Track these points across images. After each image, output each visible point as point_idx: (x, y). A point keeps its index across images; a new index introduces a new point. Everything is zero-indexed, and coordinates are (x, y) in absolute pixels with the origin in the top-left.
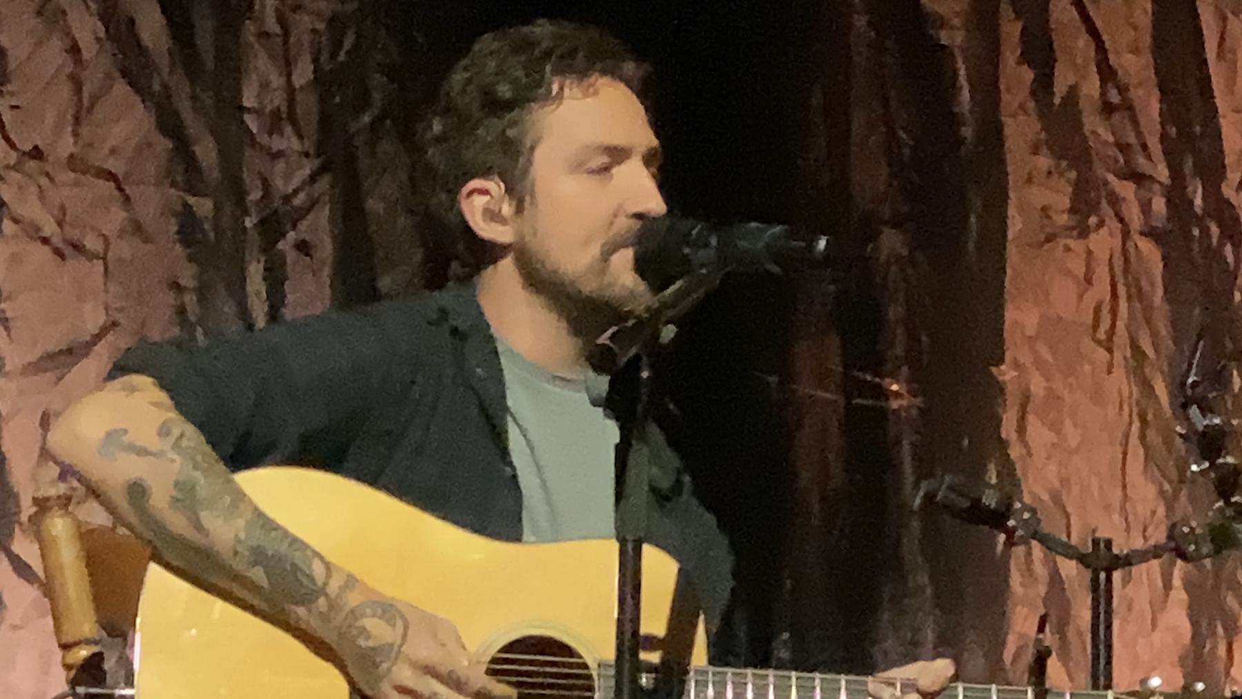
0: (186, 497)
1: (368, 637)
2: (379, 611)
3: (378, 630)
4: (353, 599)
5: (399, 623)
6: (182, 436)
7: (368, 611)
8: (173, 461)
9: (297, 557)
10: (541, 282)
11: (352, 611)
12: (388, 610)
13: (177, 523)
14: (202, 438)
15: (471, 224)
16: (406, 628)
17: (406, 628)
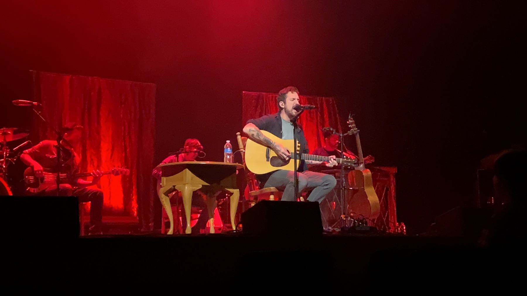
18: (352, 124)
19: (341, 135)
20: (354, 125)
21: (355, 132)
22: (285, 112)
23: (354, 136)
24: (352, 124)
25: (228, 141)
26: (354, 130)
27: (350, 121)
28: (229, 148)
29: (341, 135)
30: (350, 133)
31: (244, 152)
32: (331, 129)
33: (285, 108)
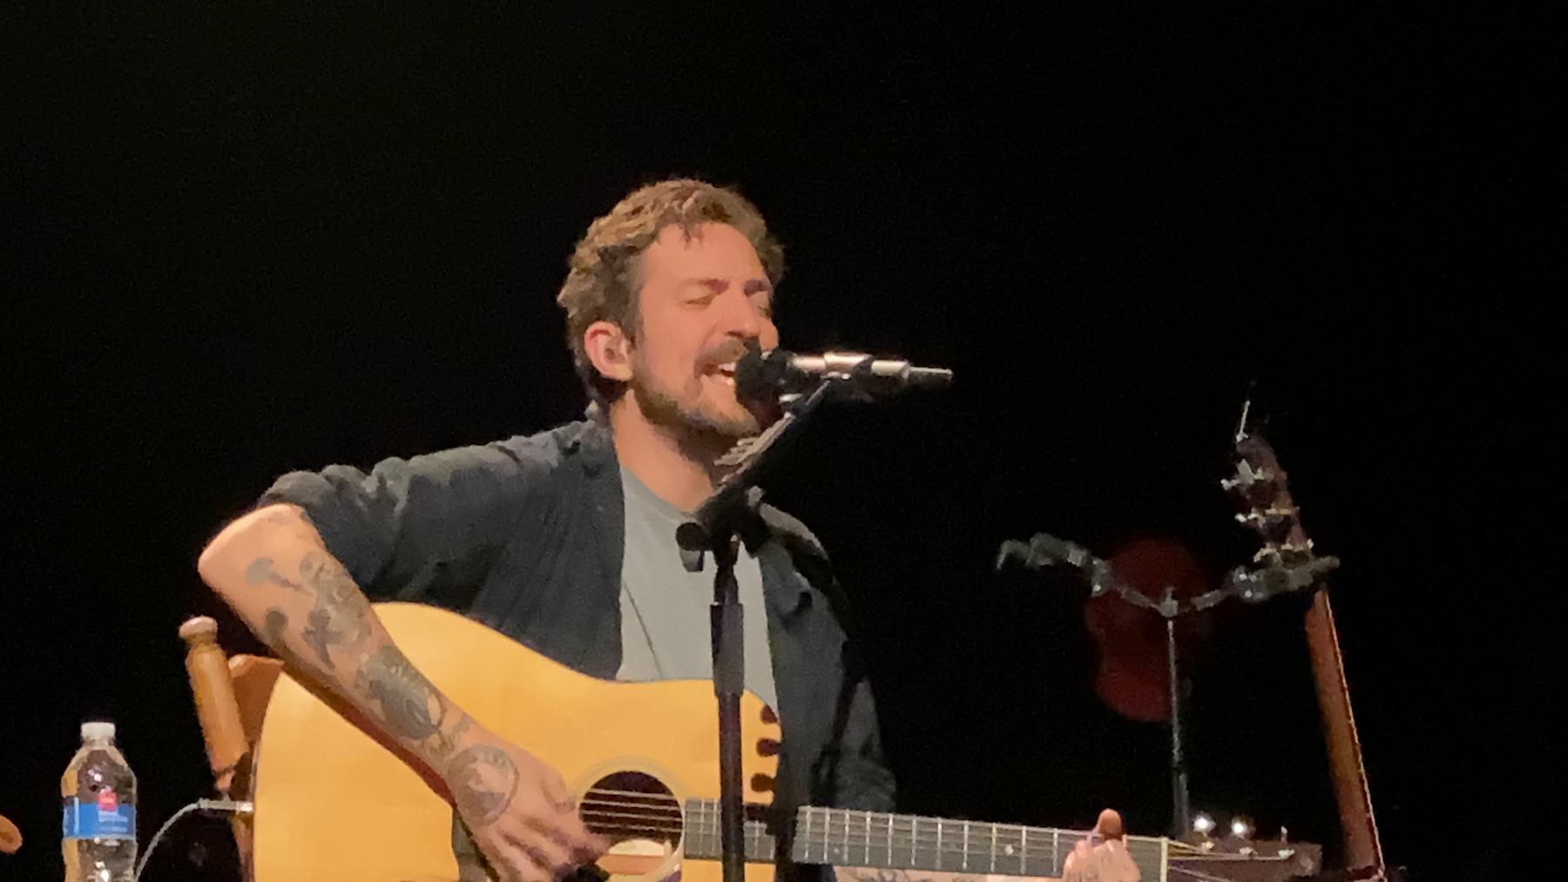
0: (319, 627)
1: (479, 782)
2: (491, 758)
3: (489, 778)
4: (465, 741)
5: (511, 776)
6: (321, 569)
7: (481, 756)
8: (310, 595)
9: (417, 694)
10: (658, 413)
11: (466, 751)
12: (498, 758)
13: (307, 653)
14: (341, 568)
15: (595, 364)
16: (516, 772)
17: (517, 779)
18: (1262, 495)
19: (1169, 606)
20: (1282, 509)
21: (1297, 578)
22: (637, 396)
23: (1288, 608)
24: (1262, 495)
25: (99, 733)
26: (1287, 558)
27: (1247, 474)
28: (106, 796)
29: (1169, 606)
30: (1248, 584)
31: (249, 820)
32: (1076, 557)
33: (637, 384)
